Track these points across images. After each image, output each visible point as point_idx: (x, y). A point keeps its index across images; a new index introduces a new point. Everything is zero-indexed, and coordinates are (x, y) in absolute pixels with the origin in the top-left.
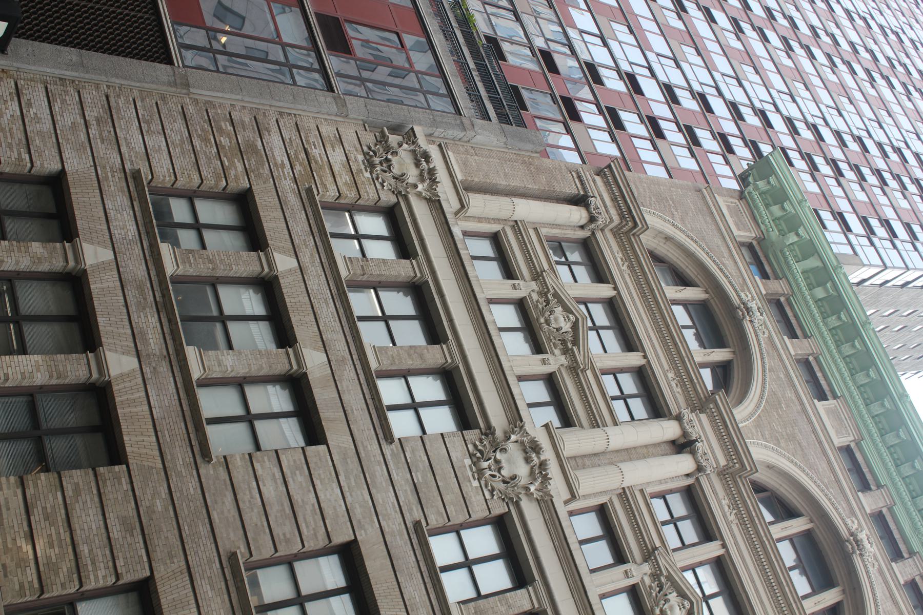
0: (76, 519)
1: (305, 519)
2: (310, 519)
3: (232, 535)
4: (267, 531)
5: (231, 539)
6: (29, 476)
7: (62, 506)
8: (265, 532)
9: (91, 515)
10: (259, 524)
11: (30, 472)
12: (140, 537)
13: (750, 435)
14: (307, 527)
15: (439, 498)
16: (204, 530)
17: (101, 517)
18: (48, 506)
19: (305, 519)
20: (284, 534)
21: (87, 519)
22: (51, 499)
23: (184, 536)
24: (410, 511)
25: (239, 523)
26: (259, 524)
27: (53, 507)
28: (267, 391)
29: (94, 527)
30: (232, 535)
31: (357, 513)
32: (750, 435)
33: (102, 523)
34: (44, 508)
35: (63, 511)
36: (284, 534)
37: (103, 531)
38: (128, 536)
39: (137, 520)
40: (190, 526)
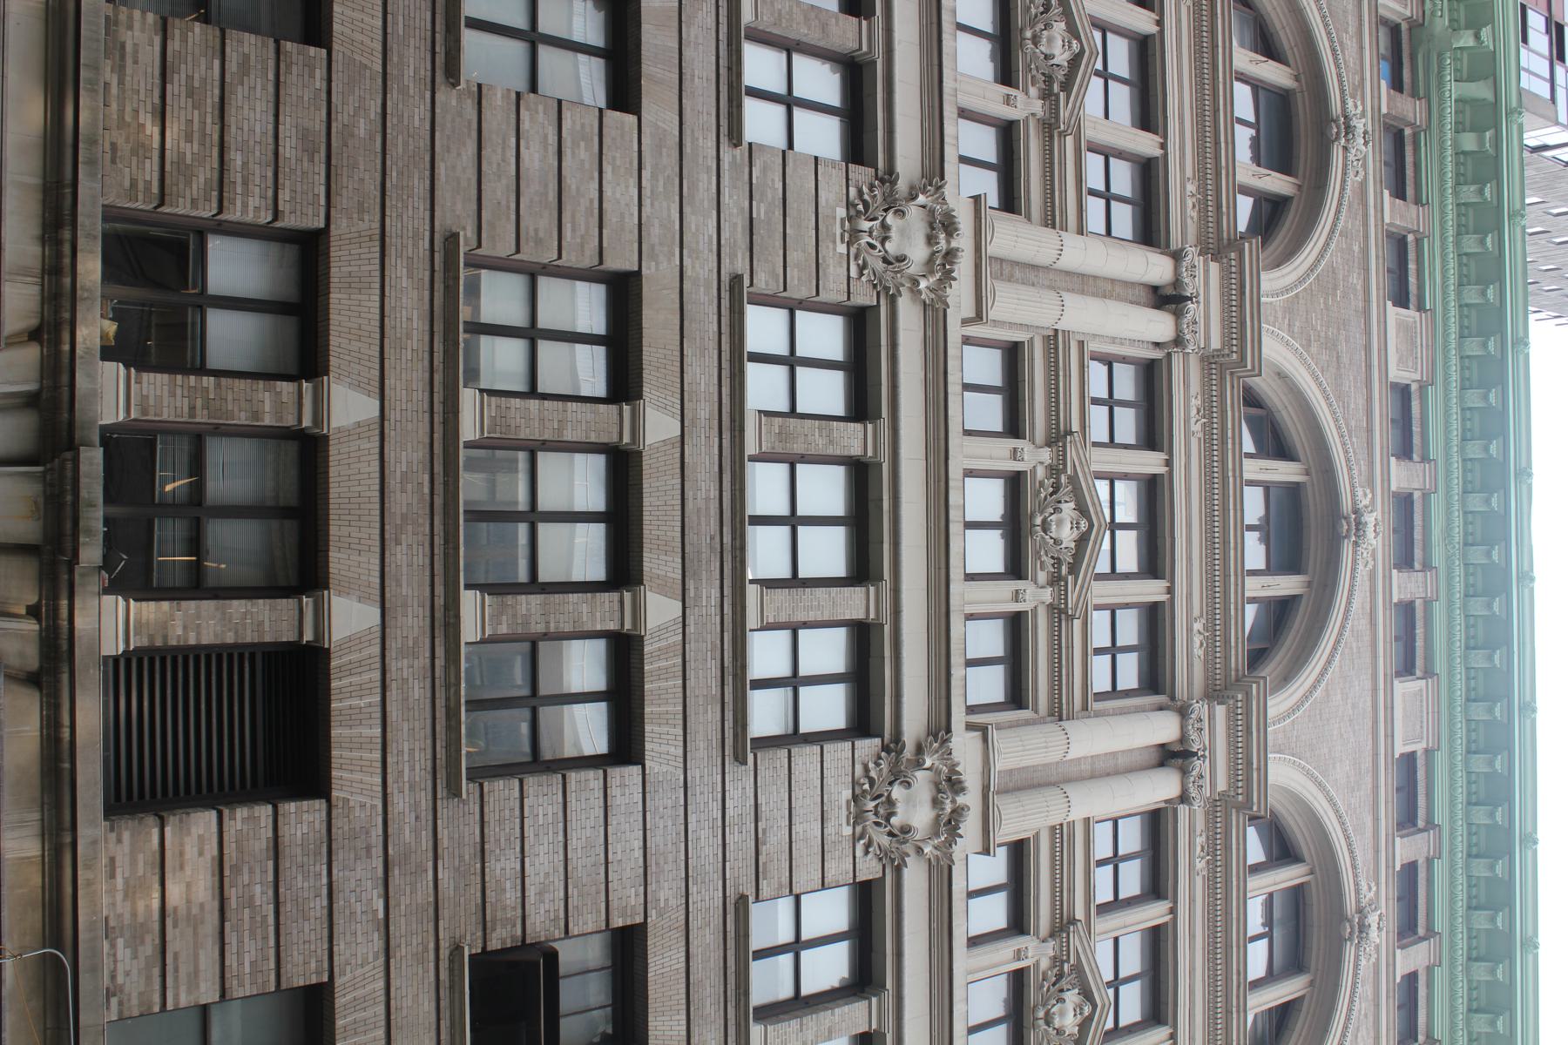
0: (233, 111)
1: (573, 217)
2: (581, 220)
3: (459, 206)
4: (513, 217)
5: (456, 211)
6: (177, 21)
7: (217, 84)
8: (508, 218)
9: (258, 109)
10: (504, 203)
11: (182, 16)
12: (323, 166)
13: (1271, 319)
14: (573, 230)
15: (781, 252)
16: (420, 186)
17: (271, 119)
18: (196, 76)
19: (573, 217)
20: (536, 230)
21: (251, 114)
22: (203, 67)
23: (388, 185)
24: (733, 256)
25: (474, 192)
26: (504, 203)
27: (204, 80)
28: (573, 292)
29: (258, 130)
30: (459, 206)
31: (654, 233)
32: (1271, 319)
33: (271, 127)
34: (190, 78)
35: (217, 91)
36: (536, 230)
37: (271, 140)
38: (305, 159)
39: (324, 140)
40: (400, 173)
